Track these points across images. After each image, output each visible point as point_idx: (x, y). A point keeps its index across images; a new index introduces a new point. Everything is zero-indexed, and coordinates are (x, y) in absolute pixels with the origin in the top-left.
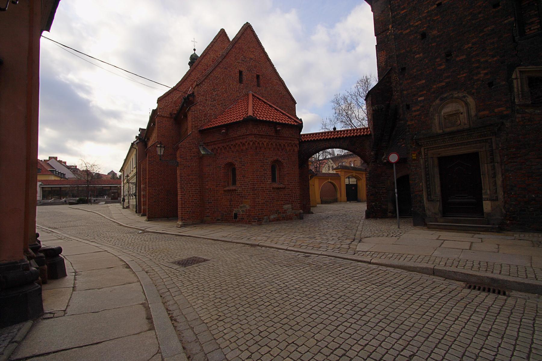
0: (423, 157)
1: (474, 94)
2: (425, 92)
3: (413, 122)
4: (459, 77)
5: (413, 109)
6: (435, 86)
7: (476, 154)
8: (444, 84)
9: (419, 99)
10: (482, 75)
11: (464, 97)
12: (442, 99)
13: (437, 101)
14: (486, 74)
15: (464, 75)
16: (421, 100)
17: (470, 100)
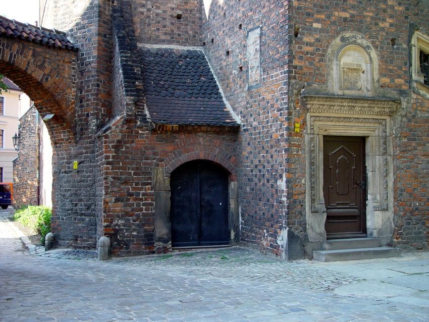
0: (309, 132)
1: (377, 48)
2: (323, 17)
3: (302, 64)
4: (365, 14)
5: (306, 39)
6: (336, 14)
7: (362, 140)
8: (347, 15)
9: (315, 25)
10: (387, 25)
11: (368, 47)
12: (343, 39)
13: (338, 40)
14: (391, 25)
15: (371, 14)
16: (317, 29)
17: (374, 54)
